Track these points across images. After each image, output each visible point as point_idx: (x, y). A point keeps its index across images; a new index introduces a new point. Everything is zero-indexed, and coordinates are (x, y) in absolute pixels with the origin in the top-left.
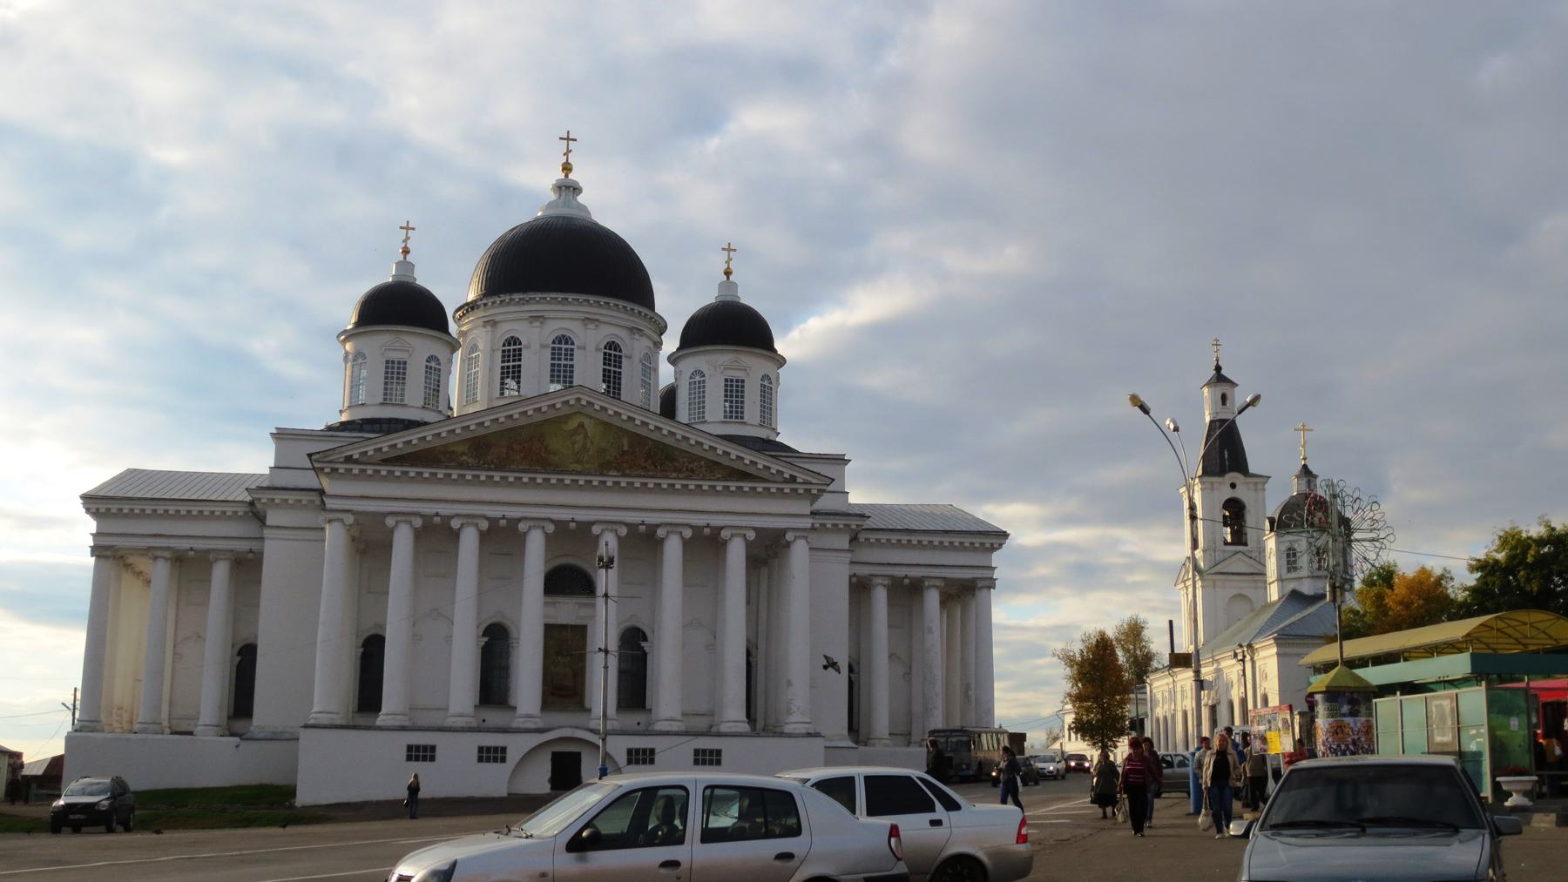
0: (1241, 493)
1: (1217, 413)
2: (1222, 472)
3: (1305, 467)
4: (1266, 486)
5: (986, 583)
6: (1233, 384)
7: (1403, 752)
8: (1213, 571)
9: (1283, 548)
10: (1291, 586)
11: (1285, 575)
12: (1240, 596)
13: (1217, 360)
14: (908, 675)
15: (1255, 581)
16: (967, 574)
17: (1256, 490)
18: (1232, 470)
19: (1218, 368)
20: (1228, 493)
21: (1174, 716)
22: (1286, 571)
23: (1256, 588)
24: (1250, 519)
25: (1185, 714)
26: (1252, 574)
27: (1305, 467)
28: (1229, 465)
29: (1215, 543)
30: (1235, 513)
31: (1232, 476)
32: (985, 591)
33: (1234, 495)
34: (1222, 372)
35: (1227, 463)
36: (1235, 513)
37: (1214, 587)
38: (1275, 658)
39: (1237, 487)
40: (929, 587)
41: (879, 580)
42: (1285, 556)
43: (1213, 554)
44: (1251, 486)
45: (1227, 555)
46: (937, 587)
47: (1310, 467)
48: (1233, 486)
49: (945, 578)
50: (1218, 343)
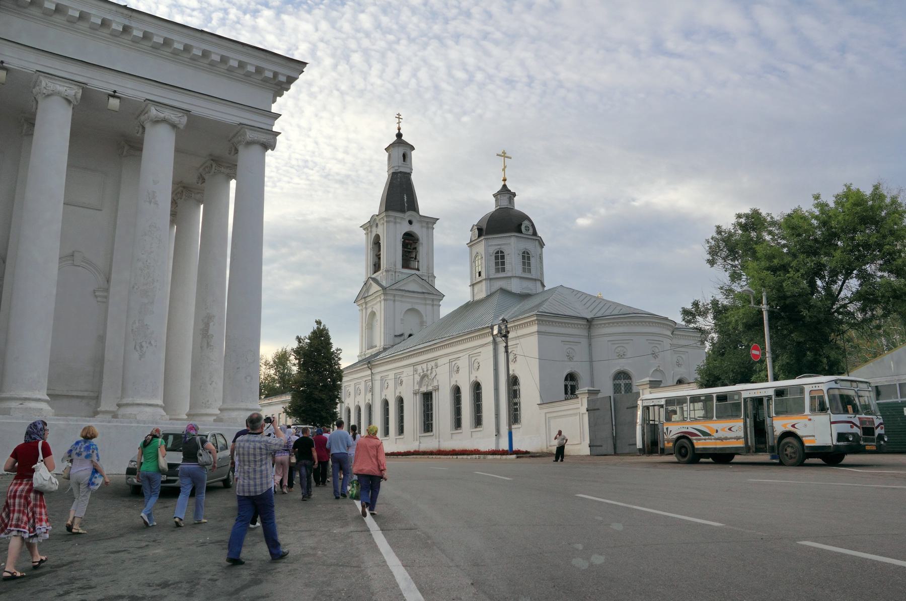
0: (416, 229)
1: (399, 166)
2: (403, 211)
3: (505, 186)
4: (434, 226)
5: (262, 137)
6: (412, 148)
7: (814, 436)
8: (394, 287)
9: (493, 250)
10: (498, 285)
11: (493, 274)
12: (412, 310)
13: (399, 129)
14: (103, 292)
15: (425, 299)
16: (232, 116)
17: (428, 228)
18: (408, 210)
19: (399, 135)
20: (406, 228)
21: (370, 408)
22: (494, 271)
23: (426, 304)
24: (422, 250)
25: (386, 403)
26: (423, 293)
27: (505, 186)
28: (407, 207)
29: (395, 266)
30: (410, 243)
31: (409, 215)
32: (257, 149)
33: (411, 230)
34: (402, 138)
35: (406, 205)
36: (410, 243)
37: (394, 301)
38: (535, 339)
39: (413, 224)
40: (157, 121)
41: (61, 88)
42: (493, 258)
43: (394, 274)
44: (424, 224)
45: (405, 276)
46: (174, 126)
47: (509, 188)
48: (410, 222)
49: (174, 202)
50: (400, 117)
